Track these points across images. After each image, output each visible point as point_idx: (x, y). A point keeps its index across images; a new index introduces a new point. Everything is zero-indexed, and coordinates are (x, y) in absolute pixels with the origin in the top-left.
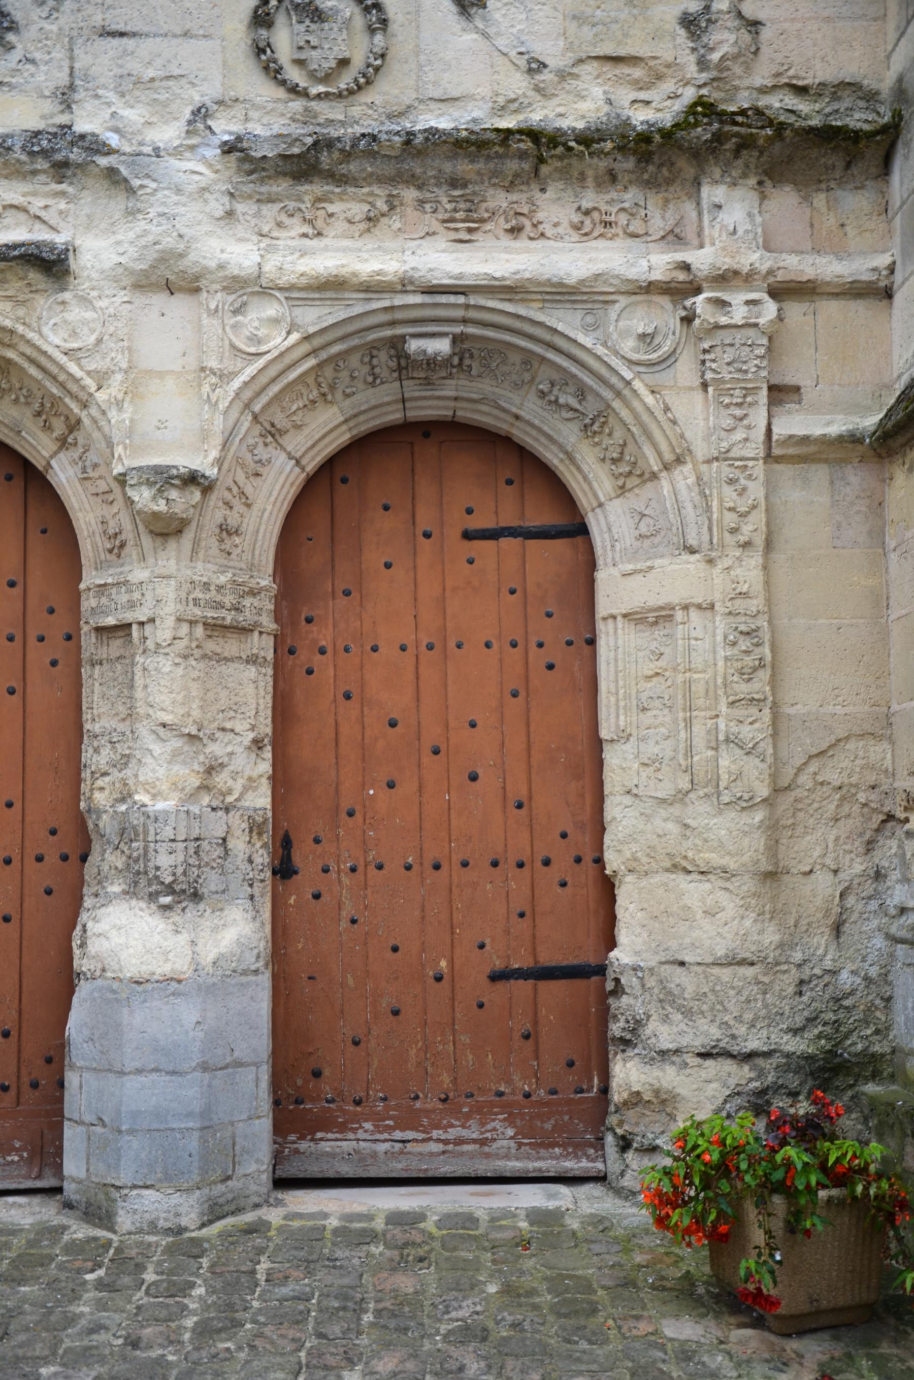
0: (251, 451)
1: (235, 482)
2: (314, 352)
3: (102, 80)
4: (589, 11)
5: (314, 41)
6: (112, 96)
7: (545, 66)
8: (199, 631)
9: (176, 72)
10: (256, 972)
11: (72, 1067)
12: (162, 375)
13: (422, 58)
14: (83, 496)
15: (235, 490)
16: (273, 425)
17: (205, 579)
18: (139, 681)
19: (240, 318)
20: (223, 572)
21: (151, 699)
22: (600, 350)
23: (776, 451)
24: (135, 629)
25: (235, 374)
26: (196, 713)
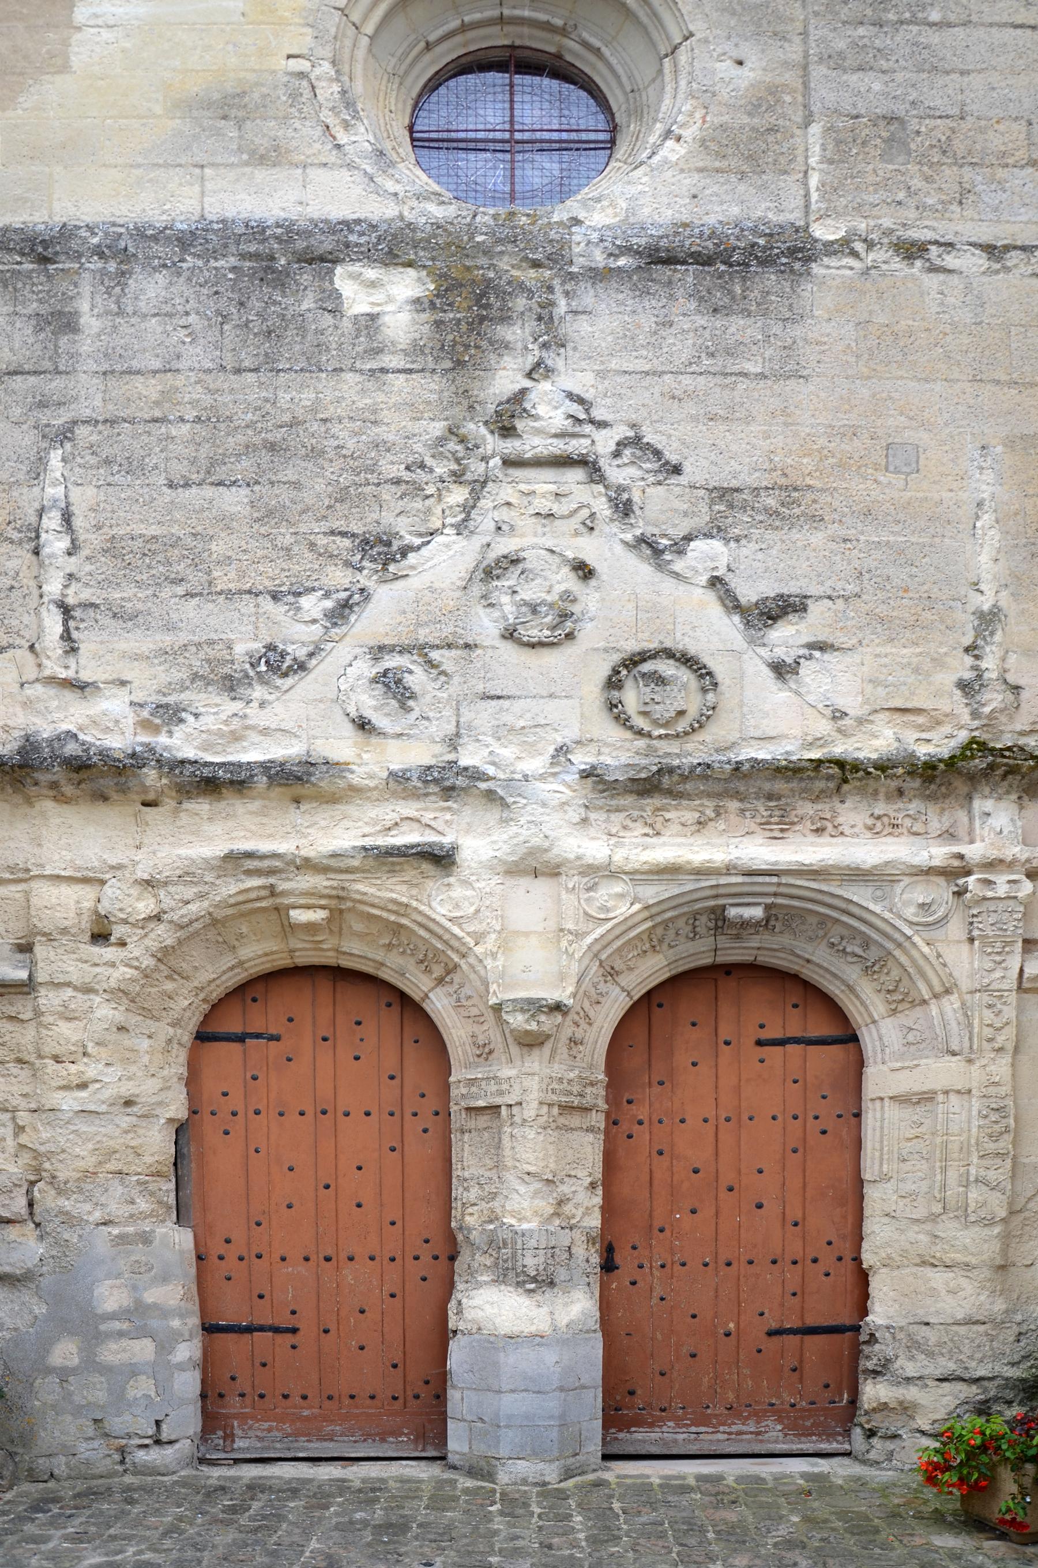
2: (651, 917)
3: (482, 729)
4: (882, 677)
5: (658, 699)
6: (490, 740)
7: (846, 715)
8: (555, 1111)
9: (543, 722)
10: (595, 1331)
11: (454, 1387)
12: (527, 934)
13: (745, 709)
19: (592, 894)
22: (887, 915)
23: (1026, 985)
25: (588, 933)
26: (552, 1166)
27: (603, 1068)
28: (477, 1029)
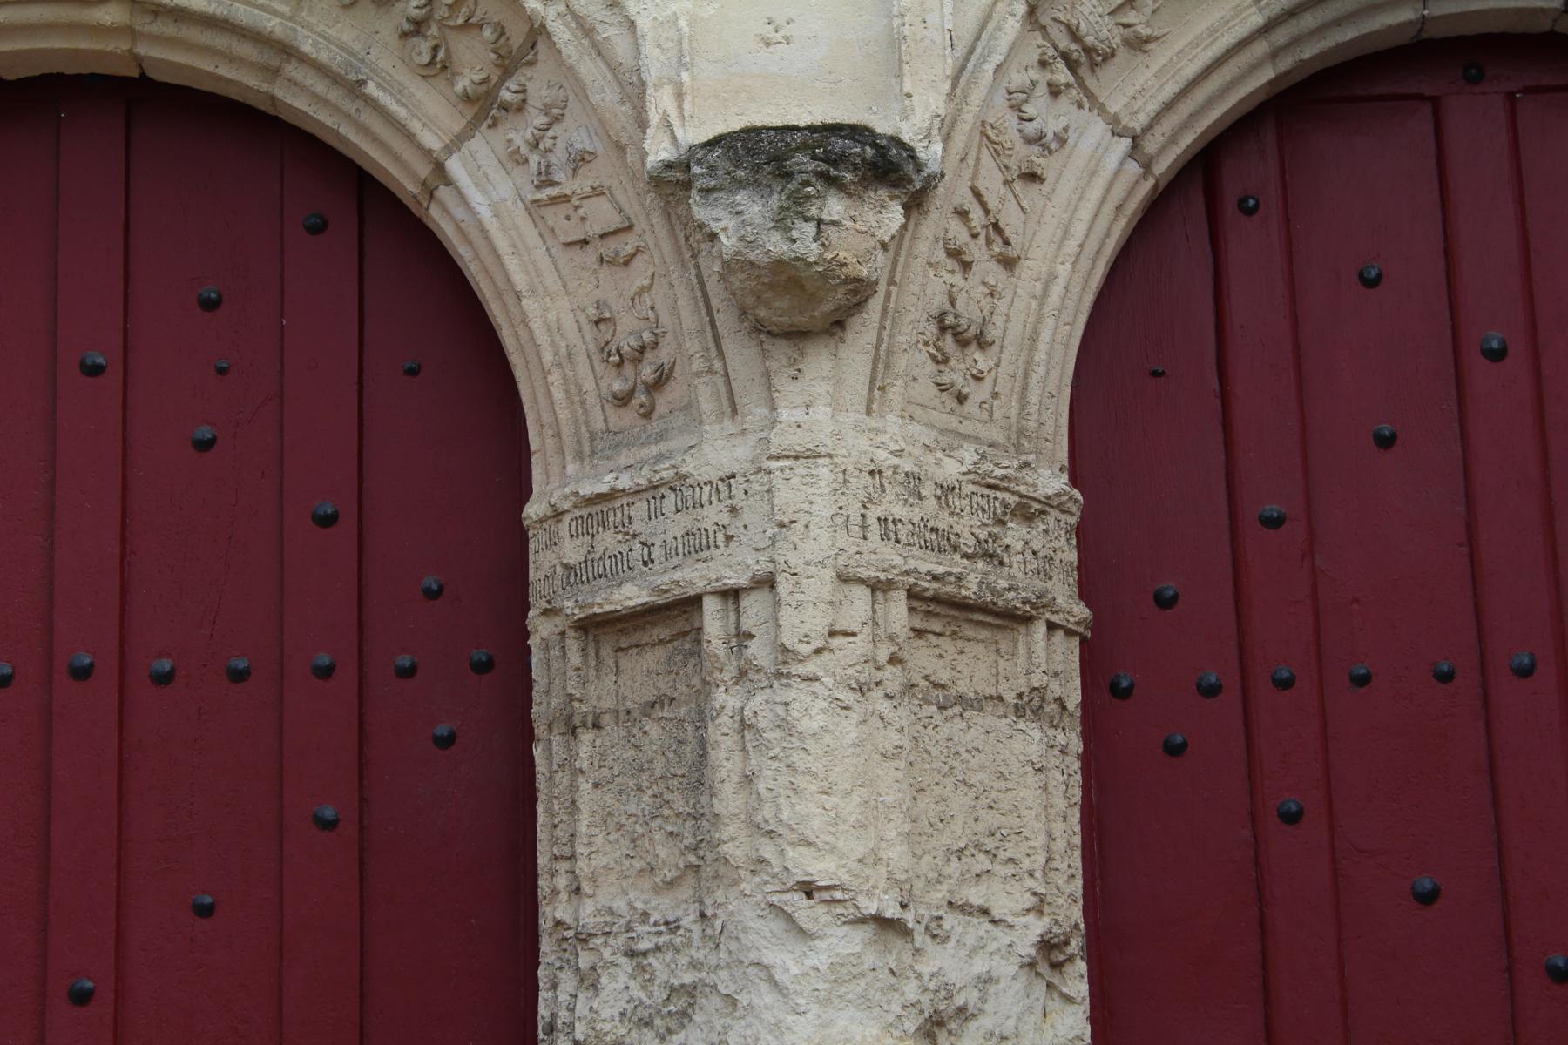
0: (1017, 108)
1: (977, 195)
8: (897, 612)
14: (540, 253)
15: (977, 215)
16: (1074, 34)
17: (907, 465)
18: (726, 760)
20: (948, 451)
21: (767, 812)
24: (713, 618)
26: (897, 854)
27: (1063, 454)
28: (614, 289)
